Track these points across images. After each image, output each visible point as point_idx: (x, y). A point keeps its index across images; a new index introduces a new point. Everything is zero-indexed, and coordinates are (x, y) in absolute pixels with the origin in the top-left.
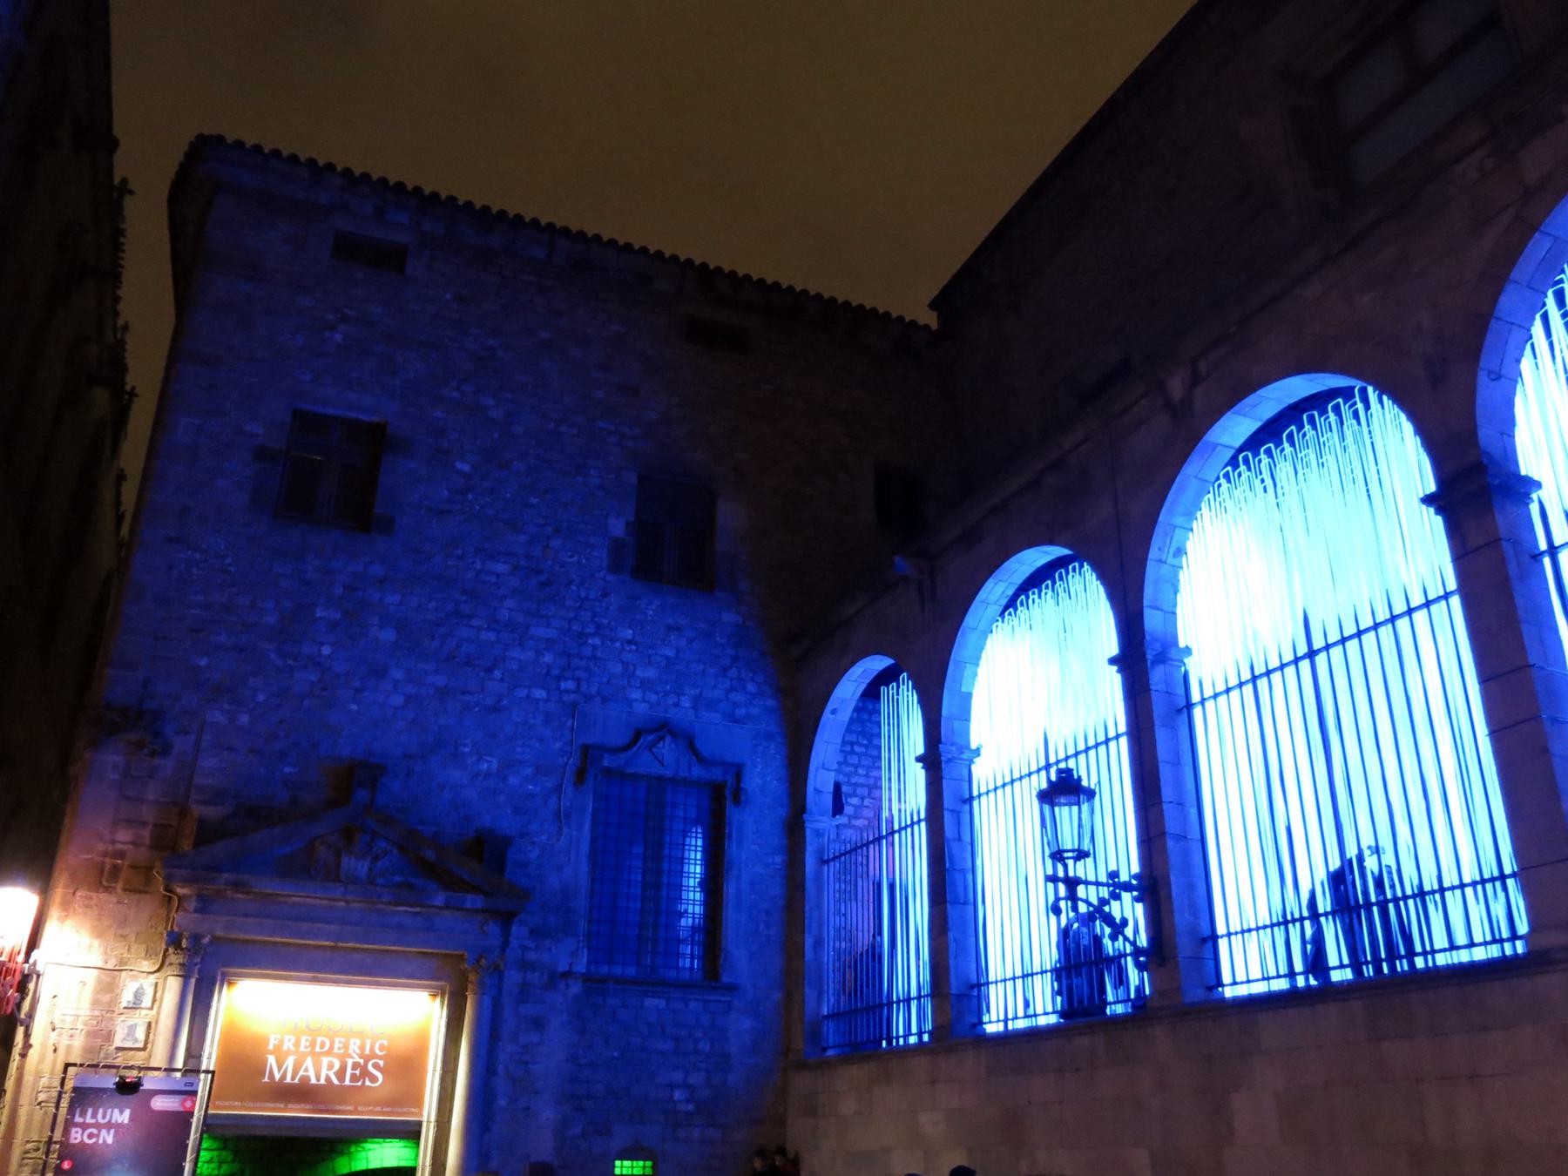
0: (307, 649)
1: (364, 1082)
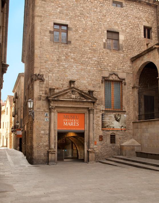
0: (61, 63)
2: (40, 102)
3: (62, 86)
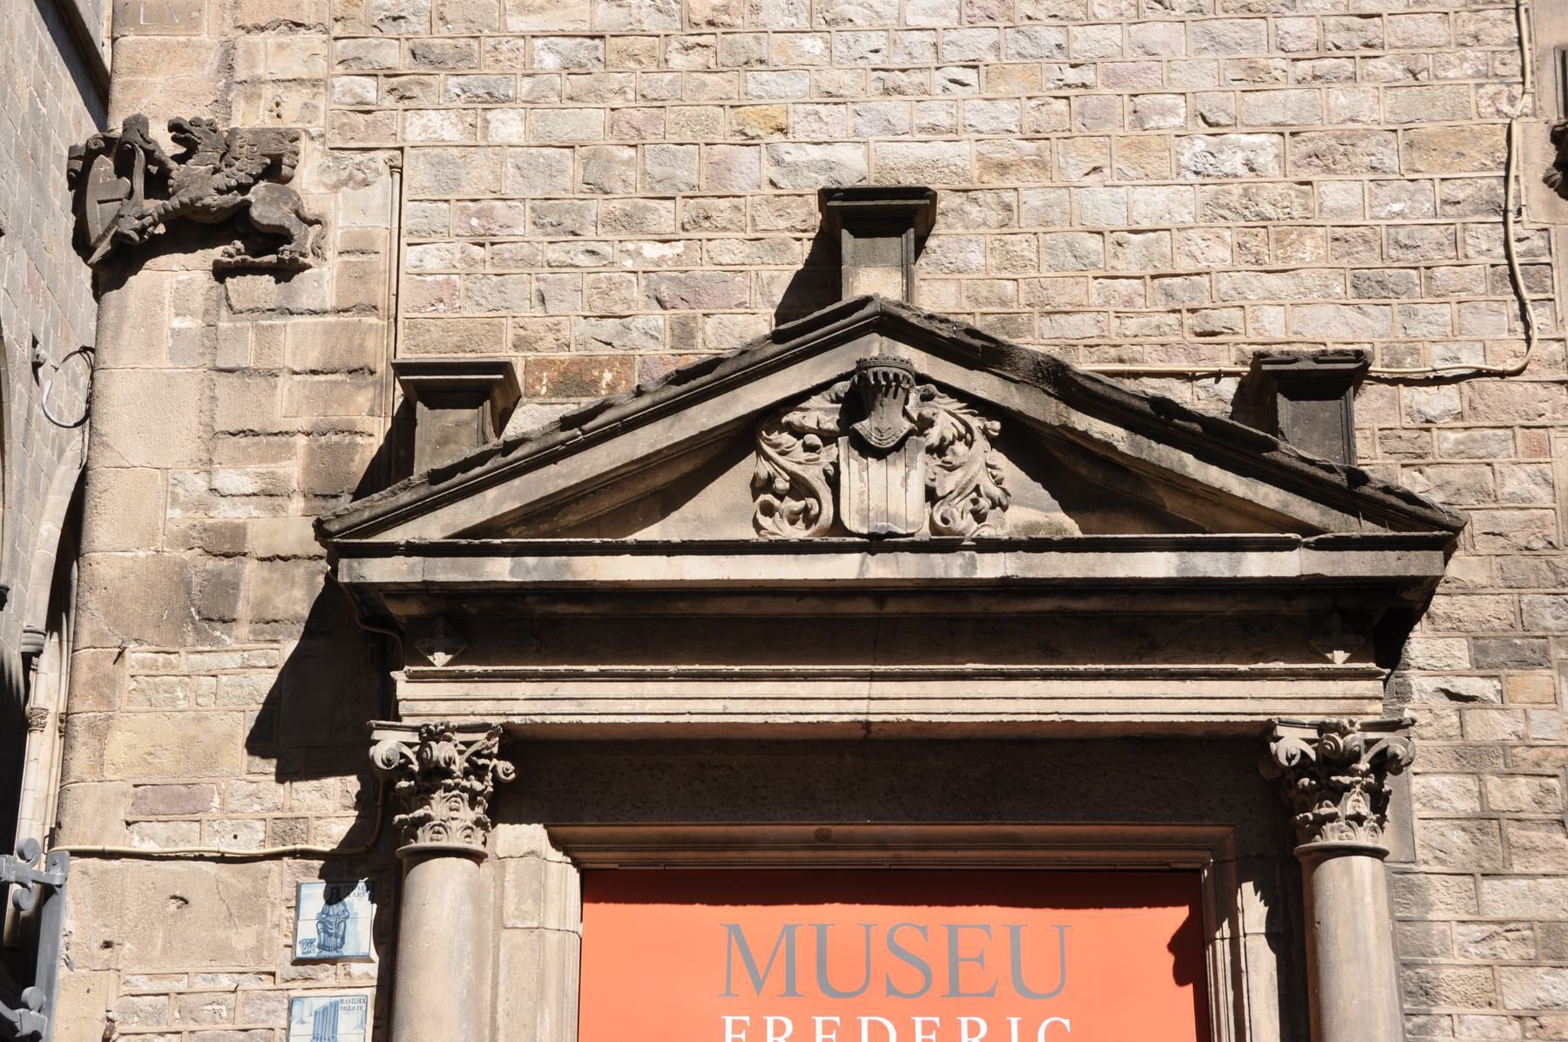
2: (210, 661)
3: (659, 319)
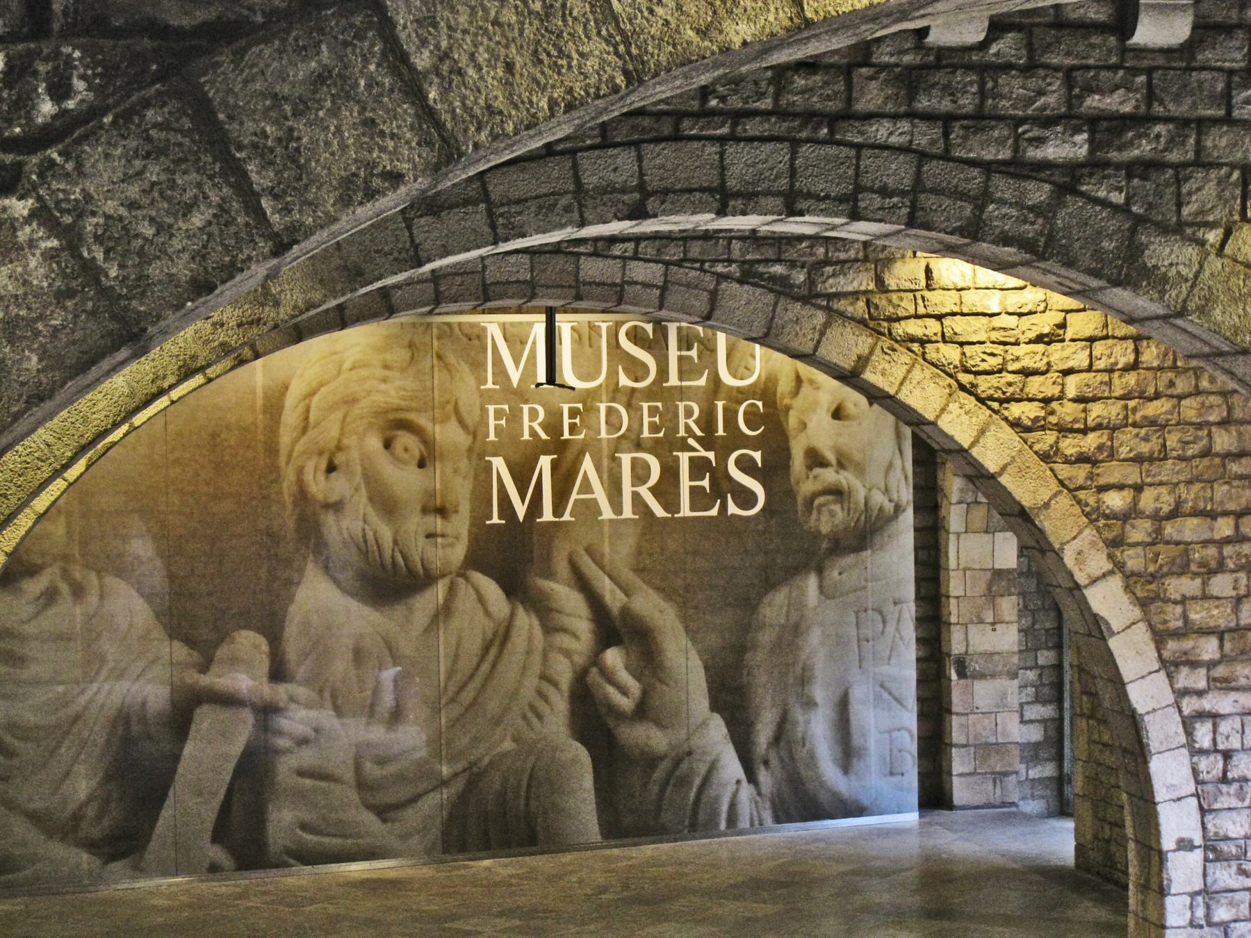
1: (724, 507)
